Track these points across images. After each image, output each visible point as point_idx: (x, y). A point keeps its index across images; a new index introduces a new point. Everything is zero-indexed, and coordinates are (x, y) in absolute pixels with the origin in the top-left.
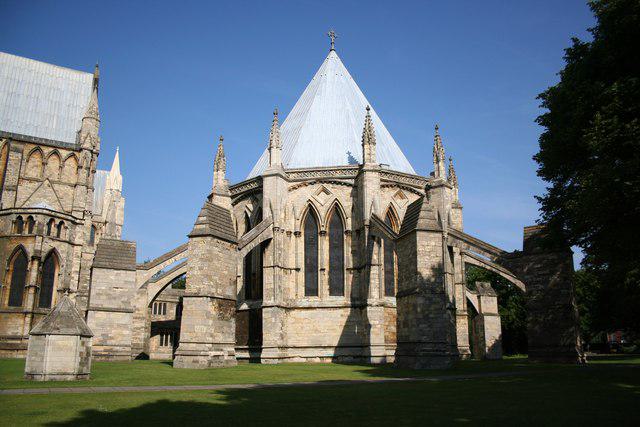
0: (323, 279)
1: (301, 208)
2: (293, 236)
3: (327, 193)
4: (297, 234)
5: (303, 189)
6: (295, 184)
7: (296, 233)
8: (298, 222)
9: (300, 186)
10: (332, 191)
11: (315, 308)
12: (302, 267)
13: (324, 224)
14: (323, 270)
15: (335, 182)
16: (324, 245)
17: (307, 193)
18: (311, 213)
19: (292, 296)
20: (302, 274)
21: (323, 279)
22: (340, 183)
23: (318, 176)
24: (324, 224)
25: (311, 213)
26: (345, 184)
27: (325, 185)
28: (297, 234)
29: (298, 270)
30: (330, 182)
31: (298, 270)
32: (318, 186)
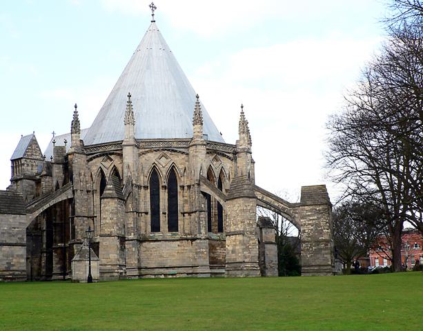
0: (164, 220)
1: (147, 170)
2: (143, 189)
4: (146, 188)
5: (149, 155)
6: (143, 150)
7: (145, 187)
8: (146, 179)
11: (160, 241)
12: (149, 211)
13: (163, 181)
14: (165, 213)
15: (173, 150)
16: (164, 196)
17: (152, 157)
18: (154, 174)
19: (143, 232)
20: (149, 216)
21: (164, 220)
22: (176, 151)
23: (161, 145)
24: (163, 181)
25: (154, 174)
28: (146, 188)
31: (147, 213)
32: (159, 154)
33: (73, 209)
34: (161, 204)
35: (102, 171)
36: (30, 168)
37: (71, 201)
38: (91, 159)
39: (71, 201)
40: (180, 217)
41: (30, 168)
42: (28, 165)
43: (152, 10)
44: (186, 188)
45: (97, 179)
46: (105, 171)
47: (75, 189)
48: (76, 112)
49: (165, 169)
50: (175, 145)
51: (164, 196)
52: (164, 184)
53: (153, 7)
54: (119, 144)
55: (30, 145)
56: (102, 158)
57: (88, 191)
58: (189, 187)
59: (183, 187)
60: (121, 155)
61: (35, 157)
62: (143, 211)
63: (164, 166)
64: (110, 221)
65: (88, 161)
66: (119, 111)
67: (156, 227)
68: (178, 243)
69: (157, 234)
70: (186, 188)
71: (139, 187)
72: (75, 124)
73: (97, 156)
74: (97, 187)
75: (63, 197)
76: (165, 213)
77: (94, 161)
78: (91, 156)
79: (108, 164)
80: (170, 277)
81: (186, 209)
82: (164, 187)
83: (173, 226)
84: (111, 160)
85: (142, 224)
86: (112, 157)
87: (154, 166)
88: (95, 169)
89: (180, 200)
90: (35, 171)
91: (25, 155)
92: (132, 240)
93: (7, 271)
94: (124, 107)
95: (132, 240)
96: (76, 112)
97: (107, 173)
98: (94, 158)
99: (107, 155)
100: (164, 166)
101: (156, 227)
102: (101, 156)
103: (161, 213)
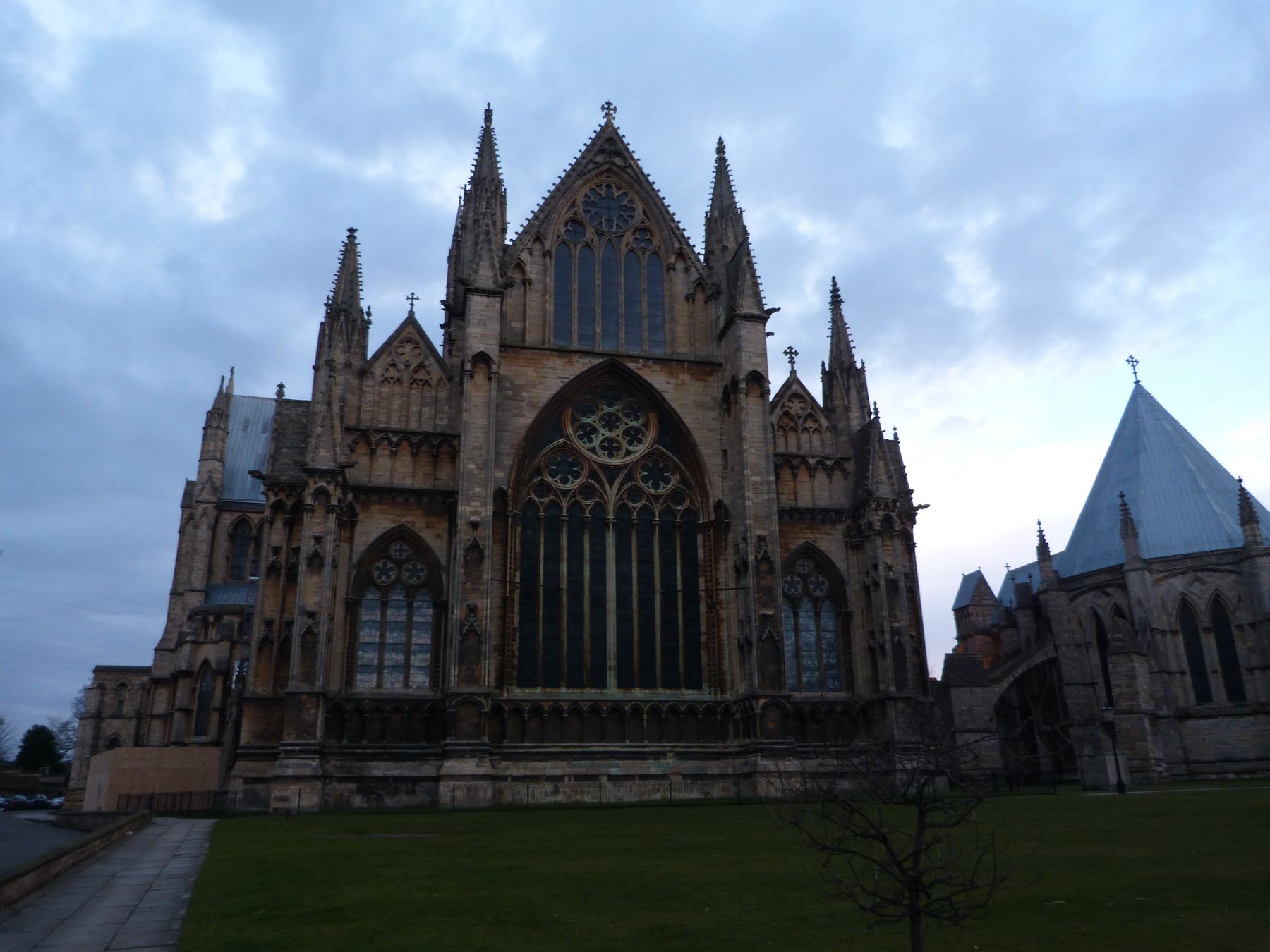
0: (1217, 684)
2: (1169, 637)
3: (1203, 582)
4: (1174, 633)
5: (1172, 580)
8: (1173, 620)
9: (1166, 577)
10: (1209, 579)
13: (1204, 619)
16: (1209, 644)
18: (1185, 607)
19: (1182, 704)
20: (1188, 679)
21: (1217, 684)
22: (1216, 571)
23: (1189, 563)
24: (1204, 619)
25: (1185, 607)
26: (1225, 571)
27: (1199, 574)
29: (1183, 673)
30: (1204, 570)
31: (1183, 673)
33: (1060, 673)
34: (1207, 657)
35: (1096, 615)
36: (981, 619)
37: (1053, 662)
38: (1075, 597)
39: (1053, 662)
40: (1246, 676)
41: (981, 619)
42: (978, 615)
43: (1134, 367)
44: (1247, 628)
45: (1090, 627)
46: (1100, 611)
47: (1057, 643)
48: (1041, 531)
49: (1202, 601)
50: (1213, 560)
51: (1209, 644)
52: (1206, 625)
53: (1133, 361)
54: (1118, 569)
55: (977, 587)
56: (1093, 593)
57: (1078, 646)
58: (1252, 625)
59: (1240, 627)
60: (1124, 587)
61: (986, 602)
62: (1175, 670)
63: (1200, 596)
64: (1128, 690)
65: (1071, 600)
66: (1110, 521)
67: (1204, 694)
68: (1251, 719)
69: (1207, 705)
70: (1247, 628)
71: (1163, 632)
72: (1043, 548)
73: (1085, 592)
74: (1091, 636)
75: (1039, 659)
76: (1215, 672)
77: (1081, 599)
78: (1074, 593)
79: (1103, 601)
80: (1247, 776)
81: (1255, 661)
82: (1207, 630)
83: (1235, 690)
84: (1108, 595)
85: (1178, 691)
86: (1110, 590)
87: (1183, 598)
88: (1083, 611)
89: (1241, 648)
90: (989, 622)
91: (972, 601)
92: (1165, 717)
93: (976, 770)
94: (1117, 516)
95: (1165, 717)
96: (1041, 531)
97: (1106, 615)
98: (1080, 594)
99: (1101, 588)
100: (1200, 596)
101: (1204, 694)
102: (1090, 590)
103: (1209, 671)
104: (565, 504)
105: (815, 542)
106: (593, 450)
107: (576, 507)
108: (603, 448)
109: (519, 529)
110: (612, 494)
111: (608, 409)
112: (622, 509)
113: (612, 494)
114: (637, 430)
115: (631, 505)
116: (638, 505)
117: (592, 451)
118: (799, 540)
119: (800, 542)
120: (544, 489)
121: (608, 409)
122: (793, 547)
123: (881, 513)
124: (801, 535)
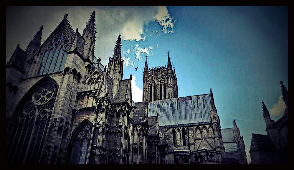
104: (25, 119)
105: (89, 119)
106: (38, 102)
107: (28, 119)
108: (40, 101)
109: (13, 128)
110: (37, 113)
111: (45, 90)
112: (39, 117)
113: (37, 113)
114: (51, 94)
115: (42, 116)
116: (44, 116)
117: (36, 103)
118: (82, 119)
119: (83, 120)
120: (23, 115)
121: (45, 90)
122: (81, 122)
123: (98, 104)
124: (85, 117)
